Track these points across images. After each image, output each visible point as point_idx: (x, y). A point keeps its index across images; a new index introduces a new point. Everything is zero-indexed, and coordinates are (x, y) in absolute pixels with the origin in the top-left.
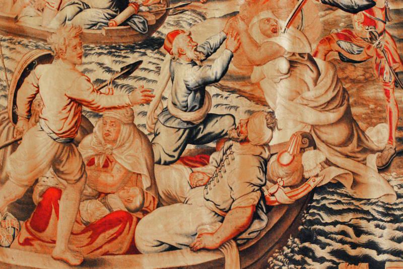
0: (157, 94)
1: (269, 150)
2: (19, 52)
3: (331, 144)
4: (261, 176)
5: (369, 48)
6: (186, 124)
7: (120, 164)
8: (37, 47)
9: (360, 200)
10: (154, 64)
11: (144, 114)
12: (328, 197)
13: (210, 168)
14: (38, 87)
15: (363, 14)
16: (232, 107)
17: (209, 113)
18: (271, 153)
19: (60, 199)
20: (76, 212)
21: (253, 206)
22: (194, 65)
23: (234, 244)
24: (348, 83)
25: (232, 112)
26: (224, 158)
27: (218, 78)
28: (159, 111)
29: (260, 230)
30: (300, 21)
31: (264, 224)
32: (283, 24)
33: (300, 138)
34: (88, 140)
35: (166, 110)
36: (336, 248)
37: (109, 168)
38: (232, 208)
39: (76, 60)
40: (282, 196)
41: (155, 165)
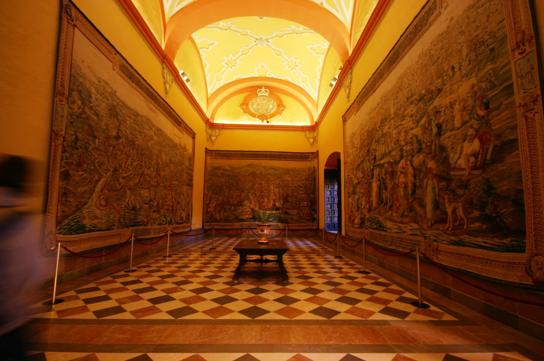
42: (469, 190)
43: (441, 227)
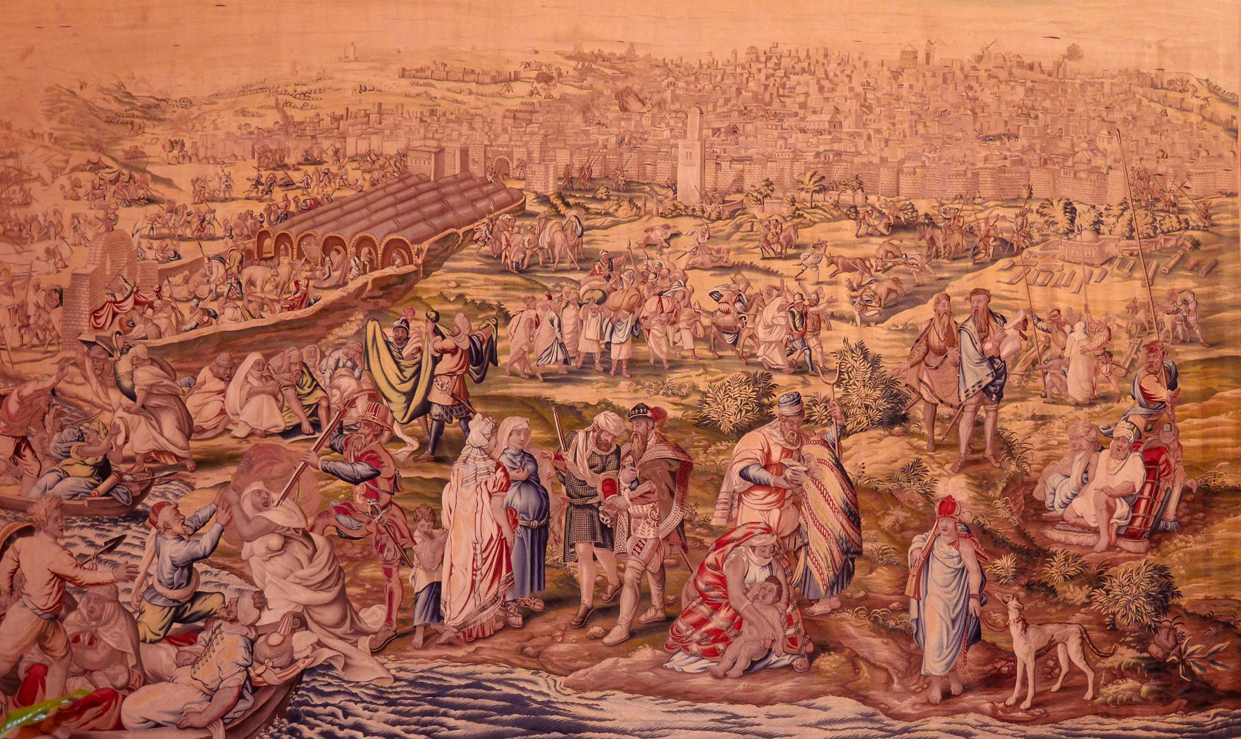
0: (142, 570)
1: (256, 630)
4: (247, 656)
5: (369, 523)
8: (16, 519)
9: (349, 682)
11: (129, 591)
13: (198, 648)
16: (221, 585)
25: (222, 590)
28: (144, 588)
31: (249, 704)
32: (276, 496)
34: (72, 617)
35: (151, 587)
39: (58, 533)
42: (1108, 592)
43: (983, 701)
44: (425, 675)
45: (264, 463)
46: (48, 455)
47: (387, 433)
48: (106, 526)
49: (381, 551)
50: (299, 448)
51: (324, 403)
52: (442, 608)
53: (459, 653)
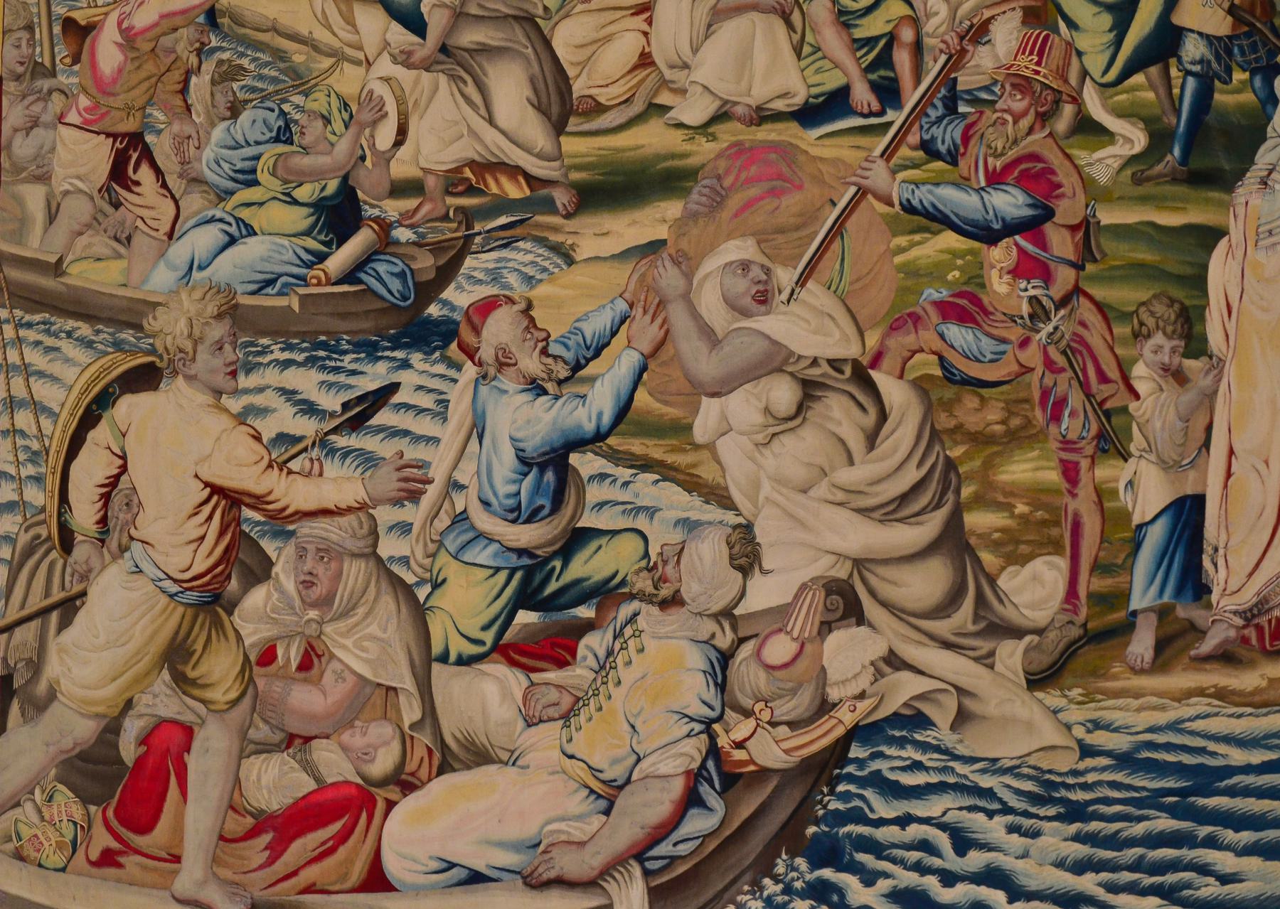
0: (438, 473)
1: (734, 628)
2: (67, 360)
3: (903, 611)
4: (711, 695)
5: (1024, 343)
6: (514, 556)
7: (340, 661)
8: (118, 345)
10: (431, 391)
11: (404, 528)
12: (1155, 699)
13: (579, 673)
14: (123, 457)
15: (1017, 244)
16: (639, 509)
17: (579, 525)
18: (741, 635)
19: (188, 751)
20: (230, 785)
21: (688, 773)
22: (539, 395)
23: (637, 870)
24: (963, 443)
25: (641, 523)
26: (617, 646)
27: (604, 429)
28: (443, 521)
29: (704, 836)
30: (837, 266)
32: (785, 276)
33: (820, 595)
34: (257, 597)
35: (461, 518)
36: (902, 886)
37: (315, 671)
38: (634, 777)
39: (221, 380)
40: (772, 751)
41: (436, 667)
44: (1160, 738)
45: (754, 191)
46: (198, 181)
47: (1068, 110)
48: (347, 361)
49: (1056, 417)
50: (843, 150)
51: (907, 35)
52: (1207, 563)
53: (1247, 680)
